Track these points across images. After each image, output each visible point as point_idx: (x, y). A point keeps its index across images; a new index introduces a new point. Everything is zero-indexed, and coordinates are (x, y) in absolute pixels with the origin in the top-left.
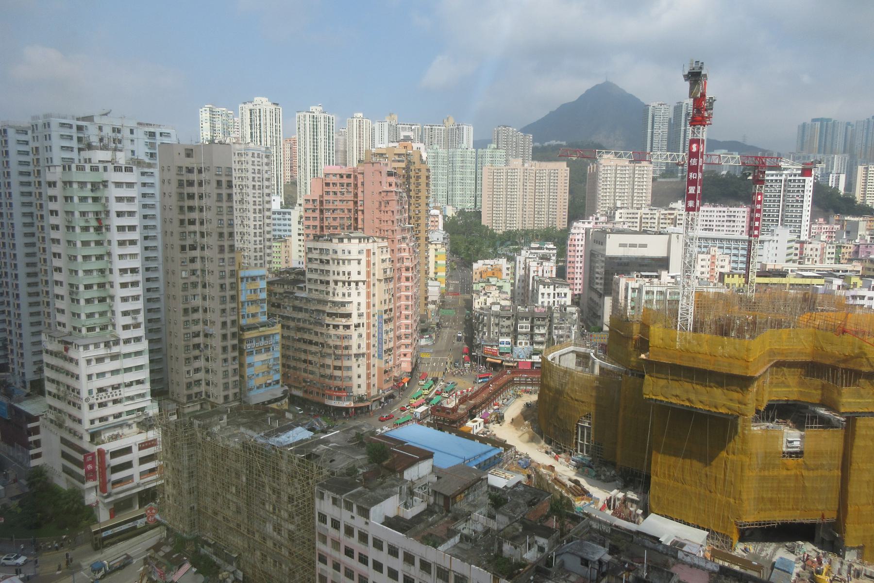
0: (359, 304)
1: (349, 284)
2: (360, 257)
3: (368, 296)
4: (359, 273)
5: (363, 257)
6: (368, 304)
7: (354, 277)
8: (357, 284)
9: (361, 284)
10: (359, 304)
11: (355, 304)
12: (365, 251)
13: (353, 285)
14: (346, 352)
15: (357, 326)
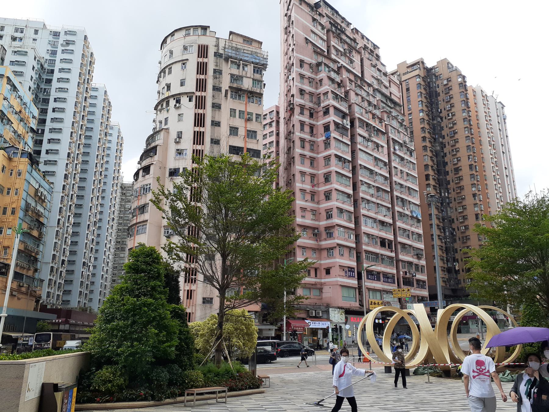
0: (180, 135)
1: (168, 104)
2: (185, 57)
3: (199, 120)
4: (182, 84)
5: (193, 59)
6: (198, 138)
7: (176, 89)
8: (178, 101)
9: (184, 100)
10: (180, 135)
11: (173, 135)
12: (195, 49)
13: (172, 102)
14: (141, 218)
15: (174, 173)
